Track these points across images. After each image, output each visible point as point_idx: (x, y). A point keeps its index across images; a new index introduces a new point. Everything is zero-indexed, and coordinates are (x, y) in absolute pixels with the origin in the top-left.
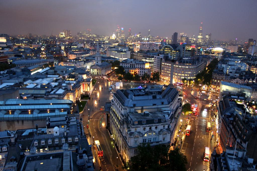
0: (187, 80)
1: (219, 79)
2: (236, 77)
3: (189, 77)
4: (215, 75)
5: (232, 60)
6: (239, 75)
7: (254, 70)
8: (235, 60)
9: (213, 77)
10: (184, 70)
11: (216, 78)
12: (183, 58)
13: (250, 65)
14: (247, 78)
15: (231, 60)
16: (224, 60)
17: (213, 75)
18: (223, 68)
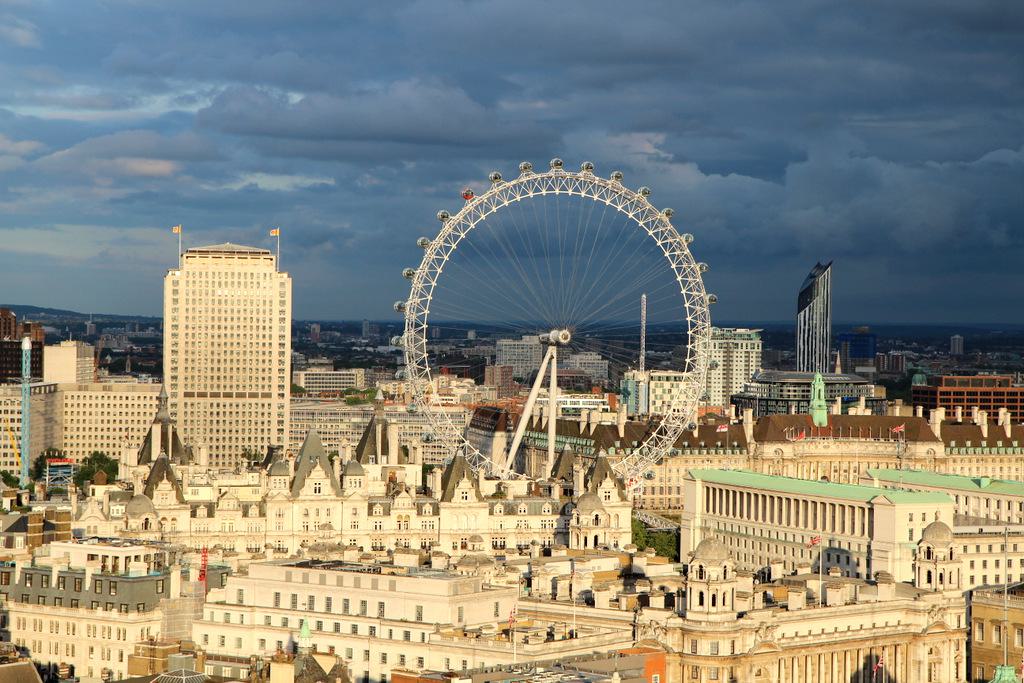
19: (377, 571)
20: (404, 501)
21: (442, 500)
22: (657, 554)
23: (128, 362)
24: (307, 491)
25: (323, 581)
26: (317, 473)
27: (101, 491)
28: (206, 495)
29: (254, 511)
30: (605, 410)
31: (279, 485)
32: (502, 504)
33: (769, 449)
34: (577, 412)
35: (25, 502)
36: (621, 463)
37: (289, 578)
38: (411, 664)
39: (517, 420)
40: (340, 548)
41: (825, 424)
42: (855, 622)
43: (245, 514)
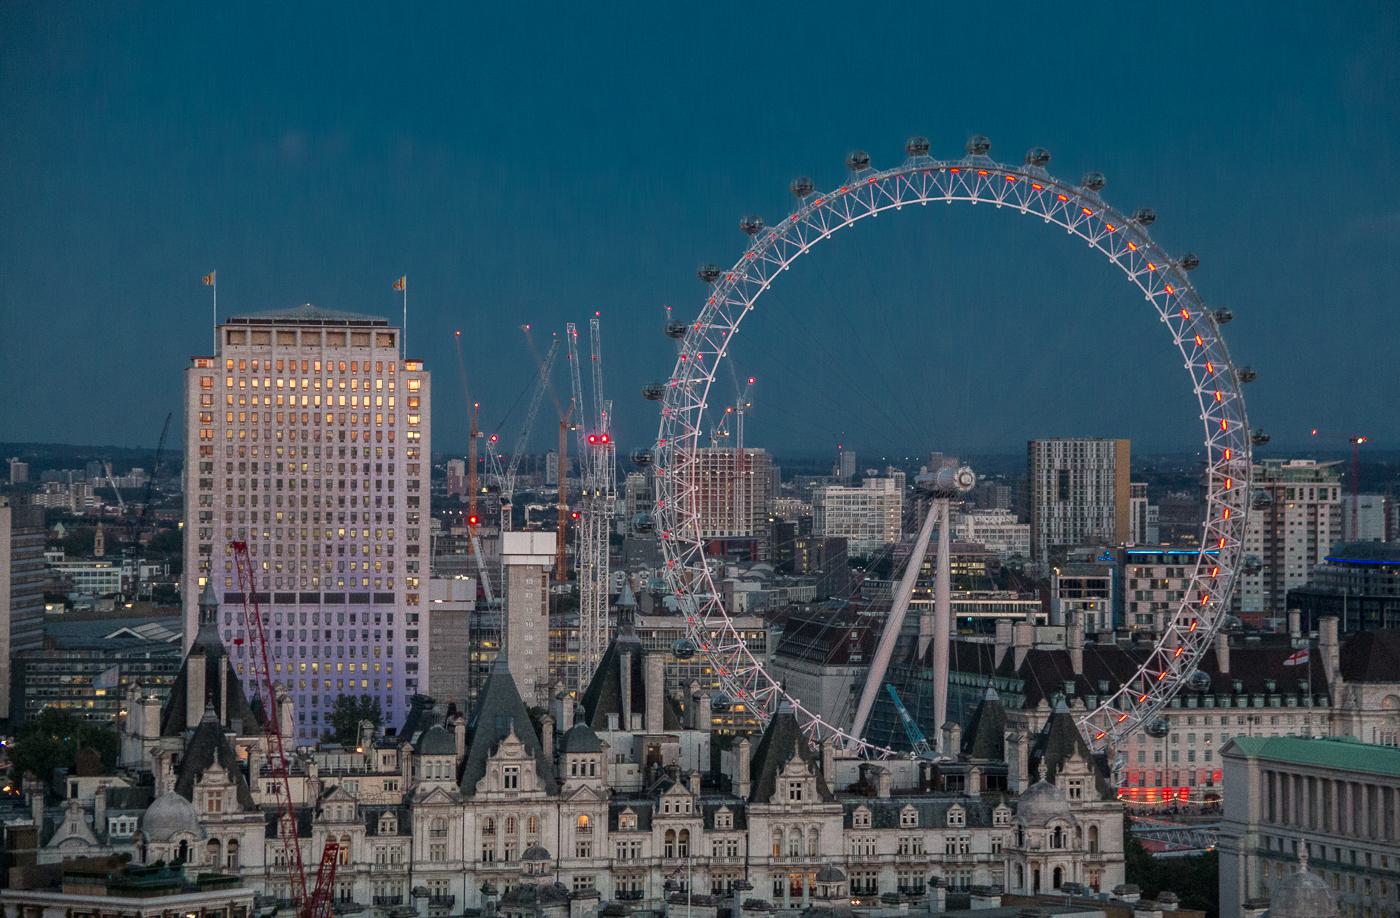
20: (678, 801)
21: (751, 800)
22: (1181, 906)
23: (100, 536)
24: (490, 786)
26: (511, 749)
28: (298, 791)
30: (1040, 622)
31: (437, 771)
32: (869, 806)
34: (989, 626)
36: (1091, 722)
43: (371, 831)
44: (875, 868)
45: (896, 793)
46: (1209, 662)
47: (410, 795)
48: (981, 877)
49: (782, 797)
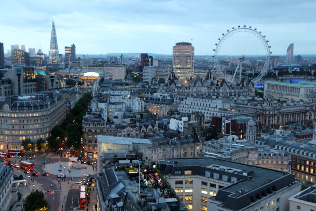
0: (32, 143)
1: (96, 131)
2: (125, 124)
3: (36, 135)
4: (87, 126)
5: (116, 93)
6: (131, 120)
7: (155, 109)
8: (121, 94)
9: (84, 130)
10: (23, 121)
11: (90, 131)
12: (20, 98)
13: (147, 100)
14: (144, 124)
15: (114, 94)
16: (101, 94)
17: (84, 125)
18: (102, 110)
19: (209, 99)
20: (214, 87)
24: (197, 85)
25: (200, 100)
27: (162, 84)
29: (188, 88)
33: (280, 78)
35: (150, 86)
37: (194, 100)
38: (215, 115)
39: (234, 72)
40: (203, 95)
41: (291, 73)
42: (296, 109)
43: (186, 89)
44: (232, 93)
45: (234, 86)
46: (266, 74)
47: (190, 86)
48: (241, 94)
49: (223, 86)
